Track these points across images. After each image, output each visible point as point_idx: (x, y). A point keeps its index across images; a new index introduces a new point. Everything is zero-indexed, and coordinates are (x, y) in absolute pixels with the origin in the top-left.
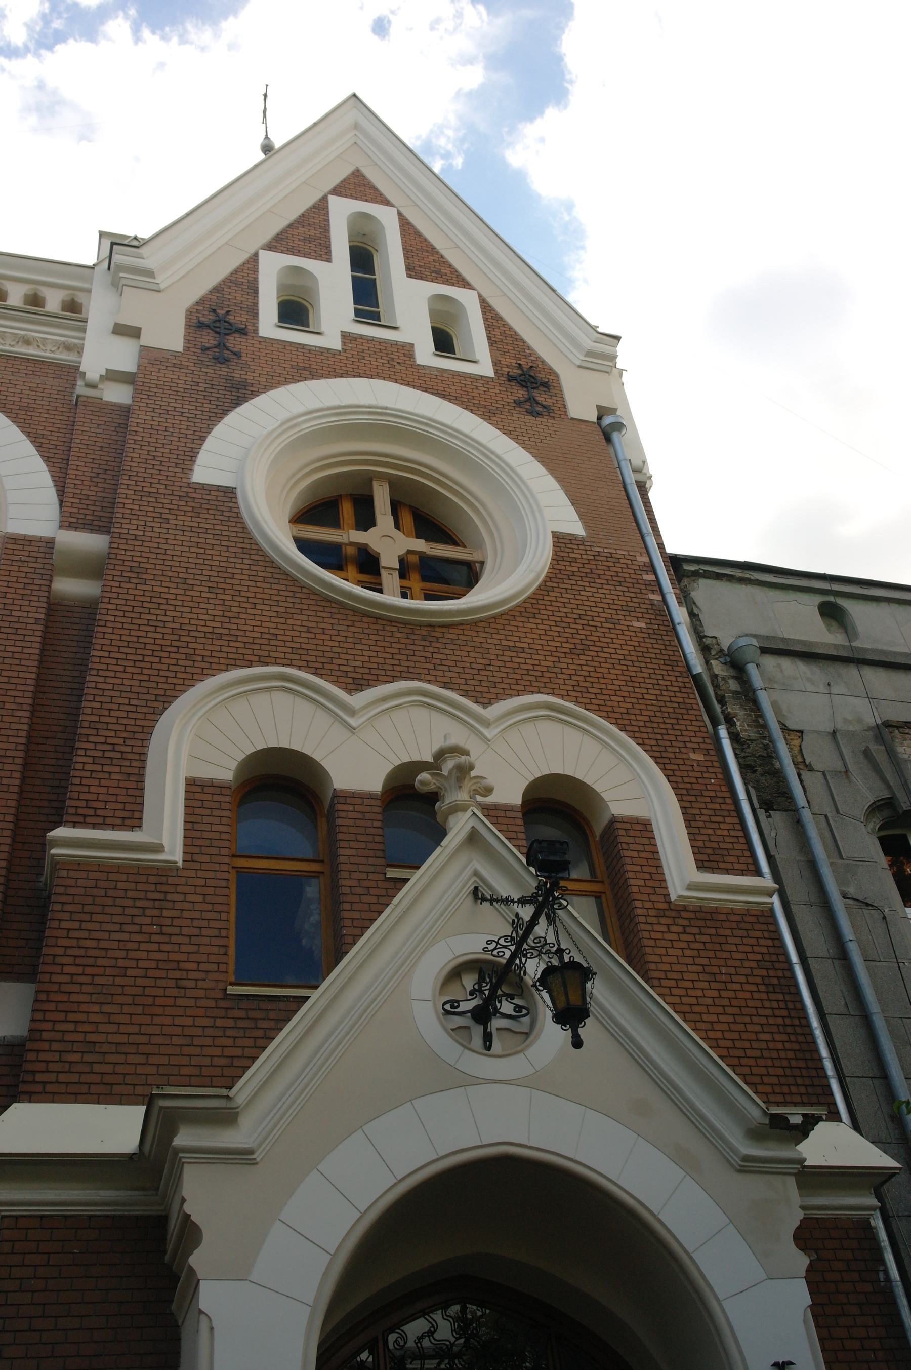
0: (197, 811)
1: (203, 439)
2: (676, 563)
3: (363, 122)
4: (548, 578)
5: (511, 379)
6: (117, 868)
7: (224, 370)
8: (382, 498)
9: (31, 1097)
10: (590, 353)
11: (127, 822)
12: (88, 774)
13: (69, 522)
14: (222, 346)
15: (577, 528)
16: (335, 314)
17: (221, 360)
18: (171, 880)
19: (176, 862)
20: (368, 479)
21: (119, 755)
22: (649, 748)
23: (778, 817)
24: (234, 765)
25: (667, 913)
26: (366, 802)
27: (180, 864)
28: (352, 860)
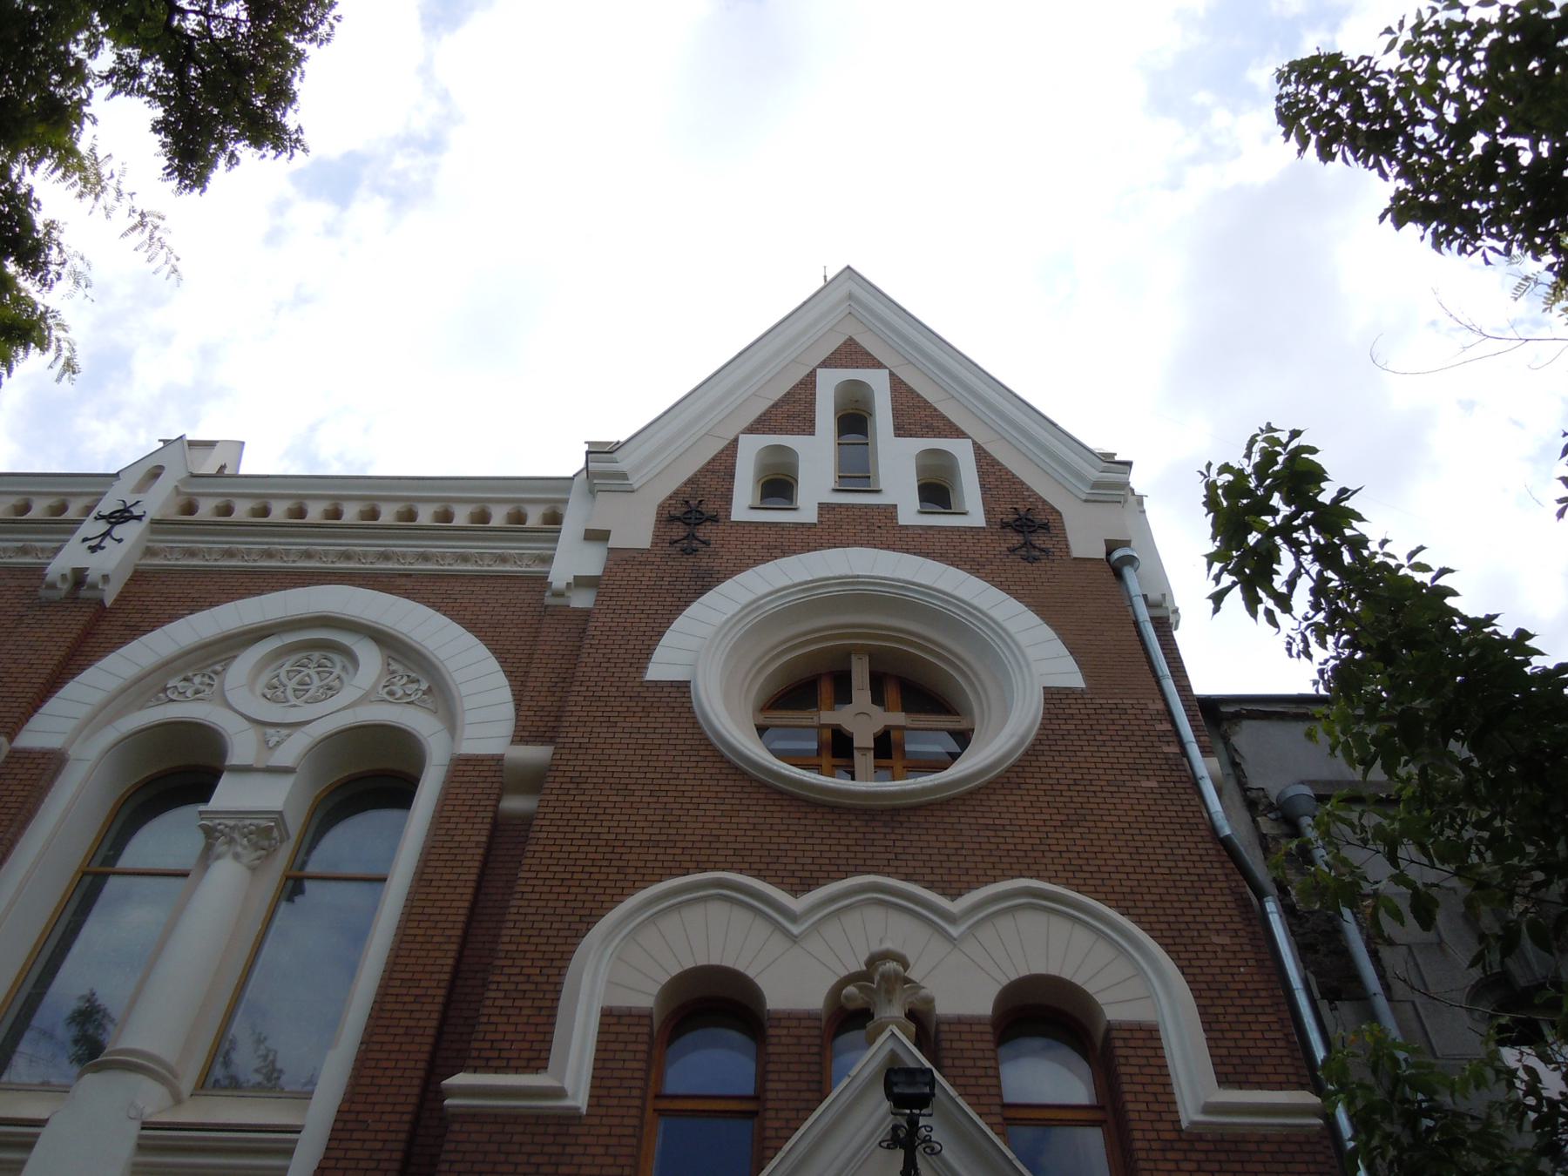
0: (611, 1046)
1: (661, 634)
3: (858, 292)
4: (1038, 741)
5: (1005, 525)
6: (515, 1118)
7: (690, 561)
10: (1096, 485)
11: (533, 1064)
12: (497, 1011)
14: (691, 537)
15: (1076, 681)
16: (817, 483)
17: (689, 552)
18: (572, 1130)
20: (846, 654)
21: (532, 987)
22: (1158, 934)
23: (1346, 1009)
24: (656, 989)
25: (1177, 1145)
26: (804, 1023)
27: (584, 1110)
28: (781, 1095)
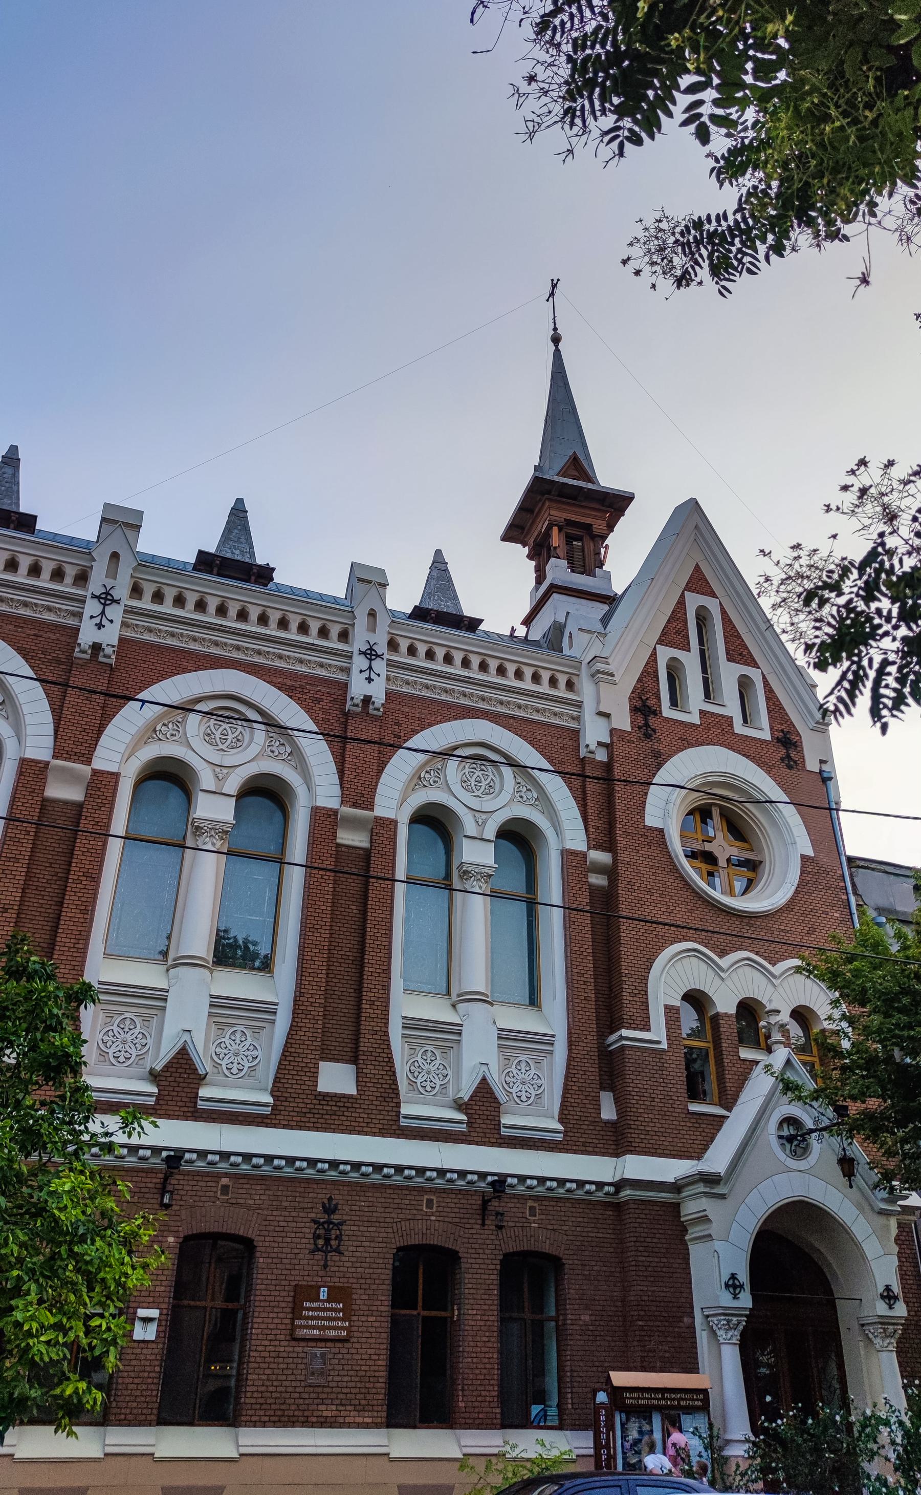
2: (850, 860)
8: (716, 813)
9: (631, 1152)
14: (647, 725)
17: (647, 736)
19: (659, 1042)
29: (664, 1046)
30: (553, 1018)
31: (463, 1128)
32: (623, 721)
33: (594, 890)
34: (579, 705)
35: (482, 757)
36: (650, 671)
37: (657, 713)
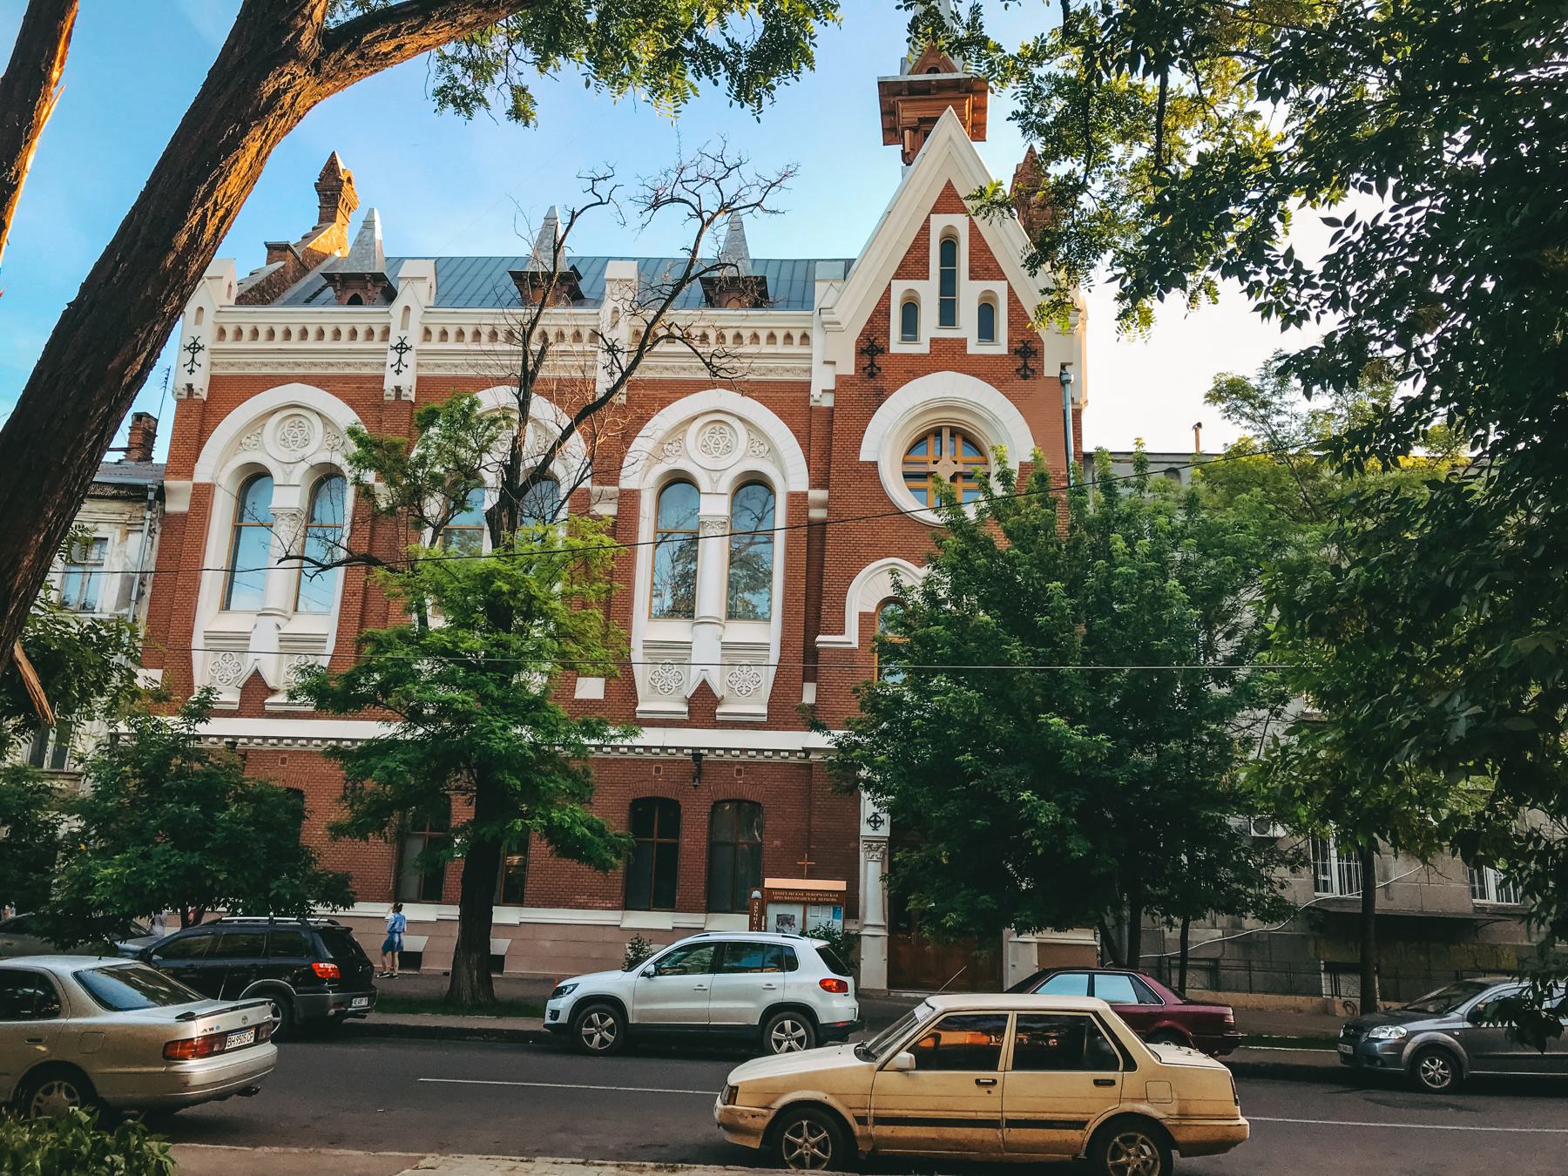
5: (1016, 352)
7: (873, 383)
13: (812, 487)
14: (872, 365)
17: (872, 375)
29: (856, 645)
30: (768, 634)
31: (686, 717)
32: (848, 367)
33: (811, 524)
34: (809, 357)
35: (718, 419)
36: (882, 310)
37: (883, 350)
